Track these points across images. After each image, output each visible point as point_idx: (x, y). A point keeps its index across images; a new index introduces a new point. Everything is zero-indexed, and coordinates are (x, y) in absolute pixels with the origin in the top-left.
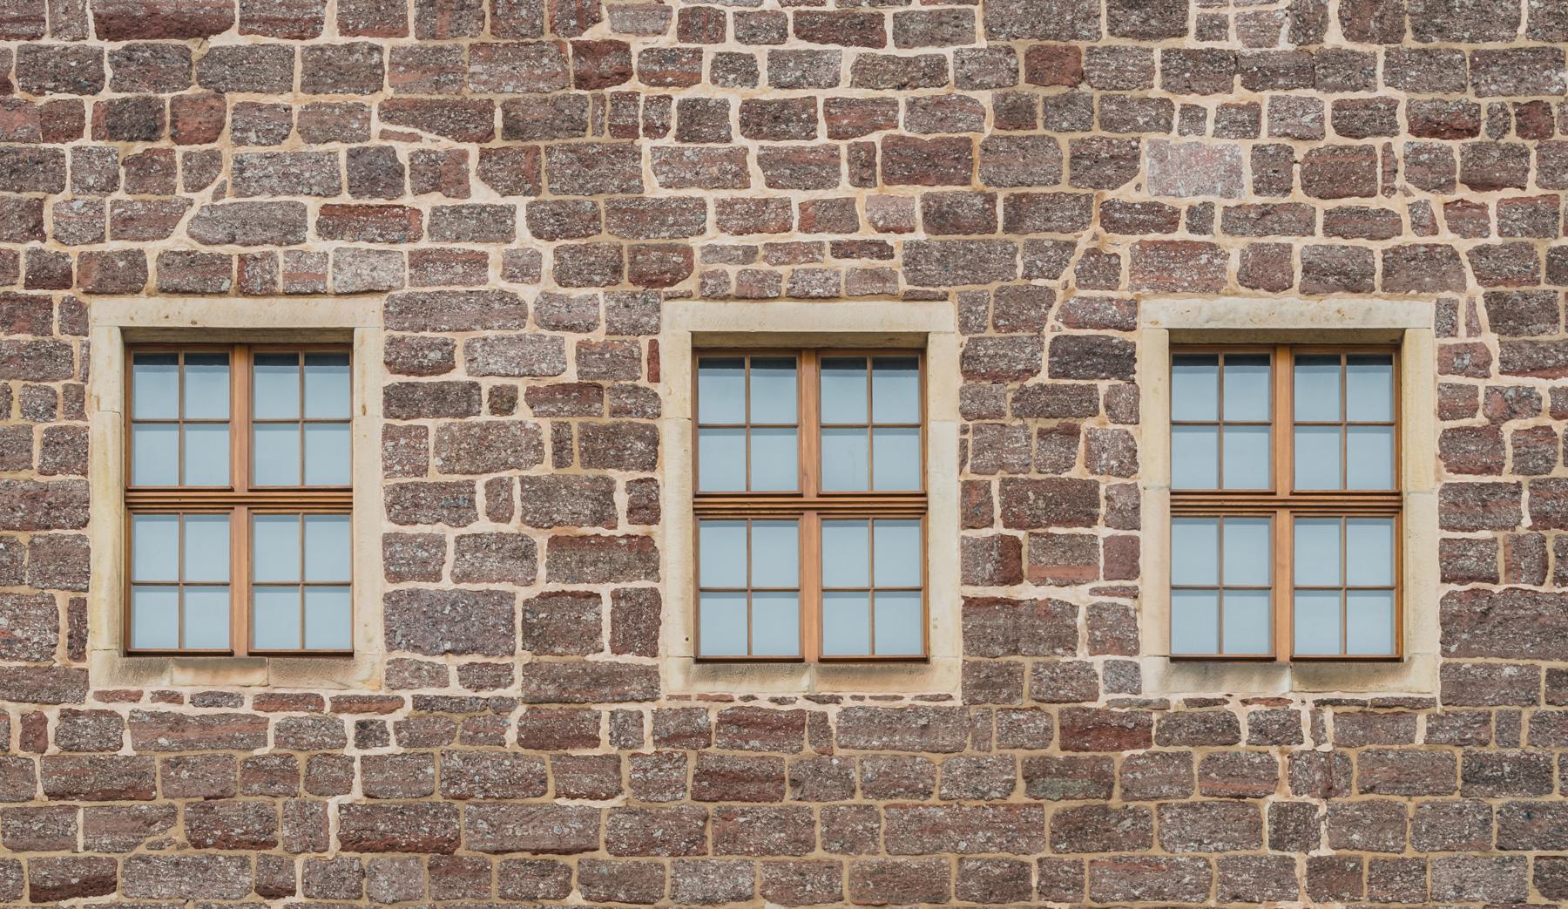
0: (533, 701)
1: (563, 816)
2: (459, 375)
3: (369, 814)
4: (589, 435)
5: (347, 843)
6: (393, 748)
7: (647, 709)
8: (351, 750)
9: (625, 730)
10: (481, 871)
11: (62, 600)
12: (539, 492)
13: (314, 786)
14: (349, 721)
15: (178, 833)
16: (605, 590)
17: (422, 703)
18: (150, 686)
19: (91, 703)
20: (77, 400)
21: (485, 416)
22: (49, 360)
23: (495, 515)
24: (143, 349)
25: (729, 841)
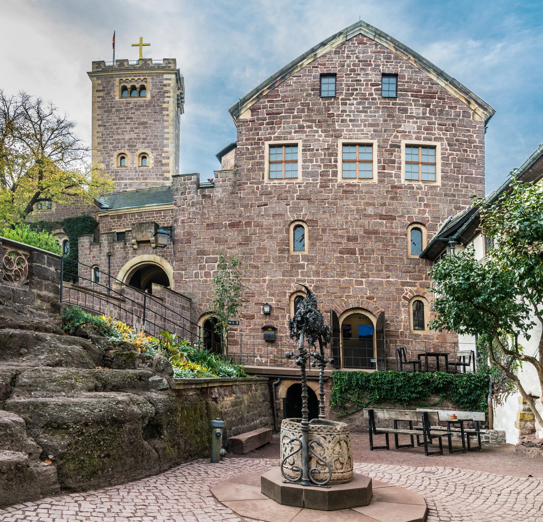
0: (321, 183)
1: (325, 196)
2: (312, 147)
3: (300, 196)
4: (328, 153)
5: (297, 199)
6: (303, 188)
7: (336, 183)
8: (298, 188)
9: (333, 186)
10: (314, 202)
11: (261, 173)
12: (321, 159)
13: (293, 193)
14: (297, 185)
15: (276, 198)
16: (331, 170)
17: (306, 183)
18: (272, 182)
19: (265, 184)
20: (263, 152)
21: (315, 151)
22: (260, 148)
23: (316, 162)
24: (271, 146)
25: (347, 199)
